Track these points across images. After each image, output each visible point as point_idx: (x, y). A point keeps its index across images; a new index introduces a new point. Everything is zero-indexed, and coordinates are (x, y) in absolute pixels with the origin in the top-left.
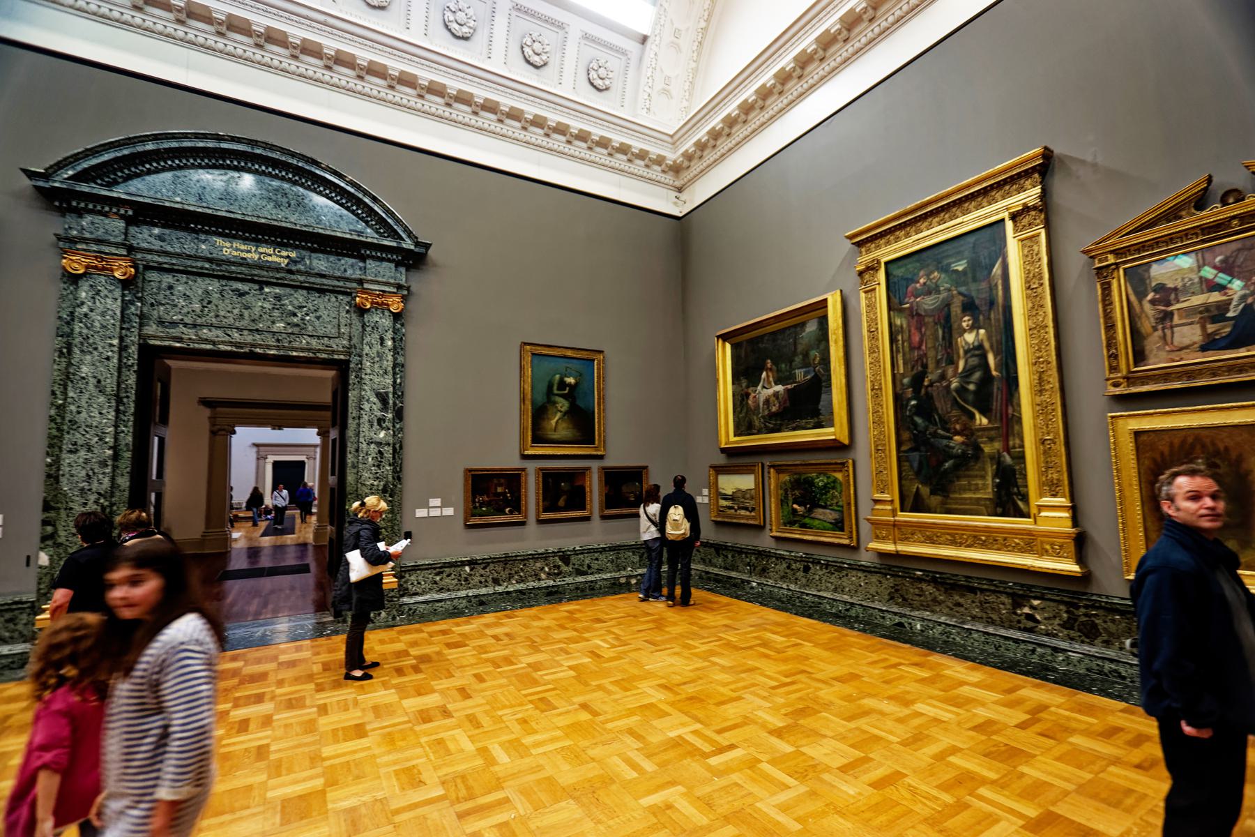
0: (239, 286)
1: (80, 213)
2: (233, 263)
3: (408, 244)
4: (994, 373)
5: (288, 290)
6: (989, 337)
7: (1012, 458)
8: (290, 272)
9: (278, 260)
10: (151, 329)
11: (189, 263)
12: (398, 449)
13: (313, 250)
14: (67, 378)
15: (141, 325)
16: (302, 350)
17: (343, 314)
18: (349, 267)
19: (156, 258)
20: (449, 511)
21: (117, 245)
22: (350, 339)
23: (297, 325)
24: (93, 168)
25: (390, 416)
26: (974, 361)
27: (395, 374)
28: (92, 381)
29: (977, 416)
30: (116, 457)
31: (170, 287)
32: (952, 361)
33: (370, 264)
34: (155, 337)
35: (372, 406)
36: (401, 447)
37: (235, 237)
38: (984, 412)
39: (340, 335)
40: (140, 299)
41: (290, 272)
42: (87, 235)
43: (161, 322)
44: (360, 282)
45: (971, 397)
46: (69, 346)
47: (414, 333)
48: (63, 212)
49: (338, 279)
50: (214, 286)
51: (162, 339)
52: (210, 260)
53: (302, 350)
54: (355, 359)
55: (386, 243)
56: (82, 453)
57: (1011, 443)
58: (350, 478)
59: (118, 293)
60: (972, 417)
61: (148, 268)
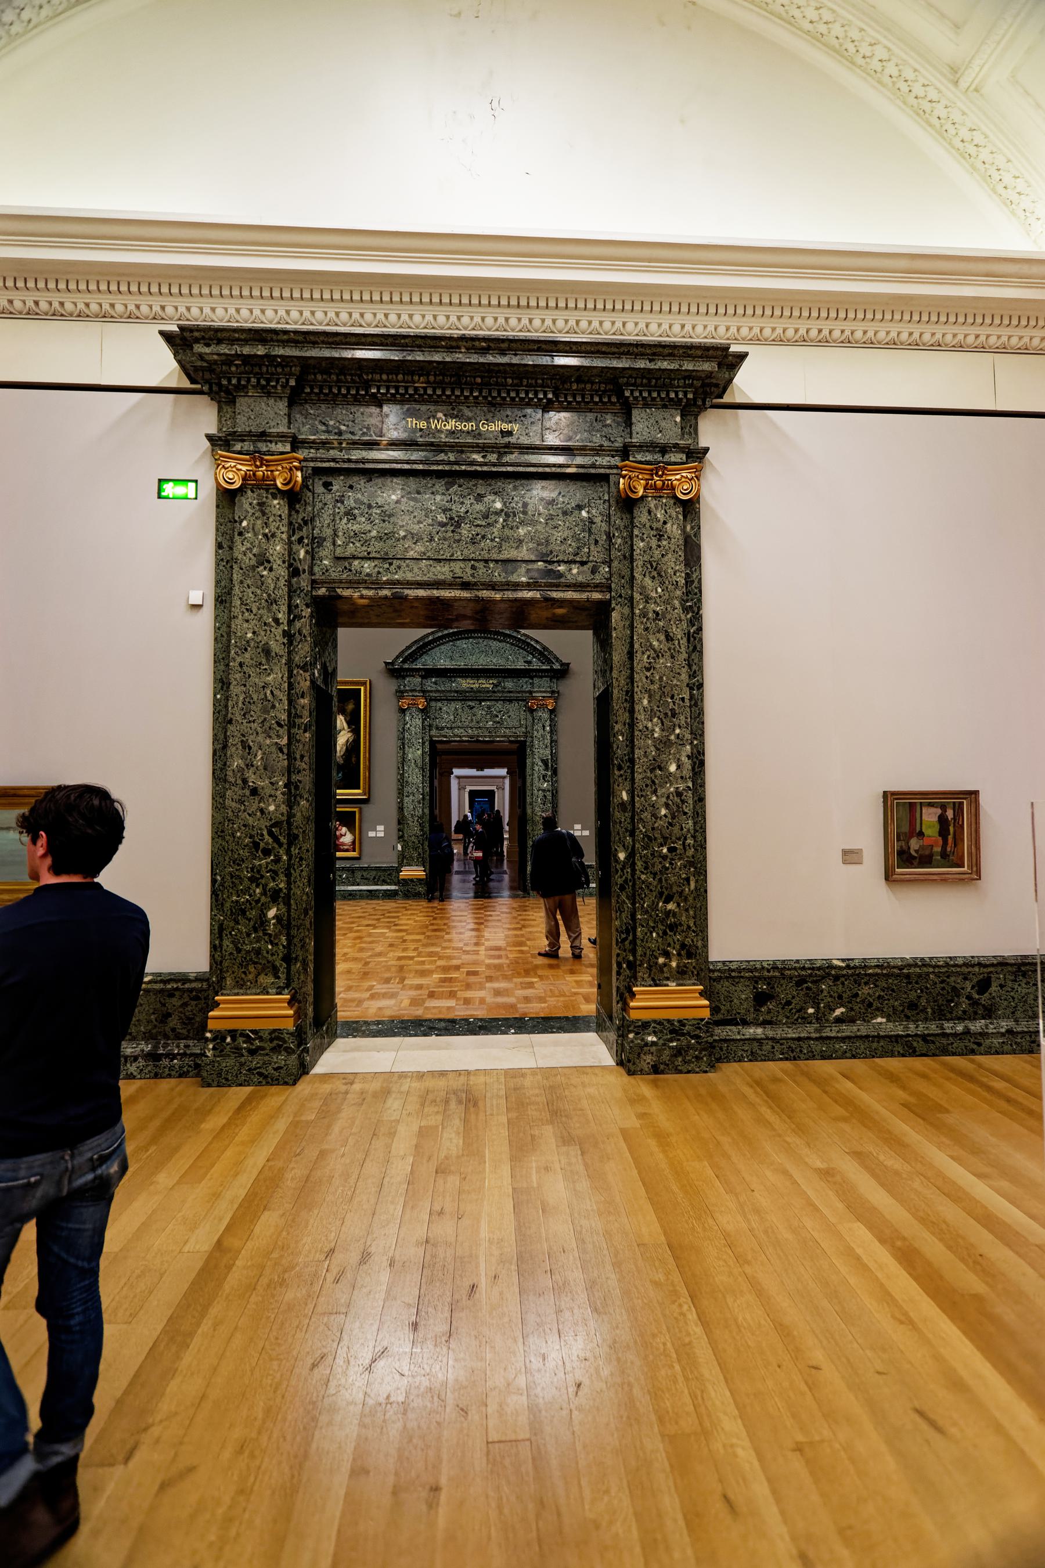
0: (470, 703)
1: (404, 678)
2: (467, 692)
3: (557, 666)
5: (493, 703)
8: (494, 692)
9: (488, 686)
10: (434, 732)
11: (448, 694)
12: (555, 793)
13: (505, 677)
14: (403, 760)
15: (430, 730)
16: (502, 736)
17: (522, 713)
18: (524, 684)
19: (434, 695)
20: (586, 833)
21: (419, 691)
22: (526, 728)
23: (499, 722)
24: (409, 655)
25: (549, 773)
27: (552, 747)
28: (413, 761)
30: (423, 799)
31: (441, 709)
33: (536, 681)
34: (436, 736)
35: (539, 767)
36: (556, 792)
37: (467, 677)
39: (521, 726)
40: (429, 717)
41: (494, 692)
42: (407, 688)
43: (437, 728)
44: (531, 692)
46: (403, 744)
47: (562, 720)
48: (397, 678)
49: (519, 692)
50: (459, 705)
51: (438, 737)
52: (456, 692)
53: (502, 736)
54: (529, 739)
55: (544, 667)
56: (411, 797)
58: (529, 811)
59: (420, 716)
61: (431, 700)
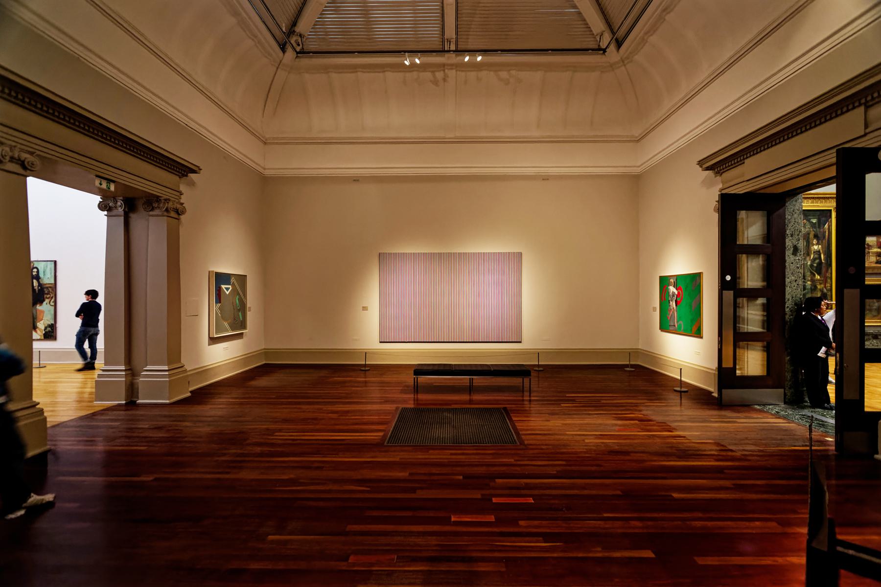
4: (823, 261)
6: (822, 249)
7: (827, 290)
26: (816, 256)
29: (816, 275)
32: (808, 254)
38: (819, 274)
45: (815, 269)
57: (827, 285)
60: (815, 275)
